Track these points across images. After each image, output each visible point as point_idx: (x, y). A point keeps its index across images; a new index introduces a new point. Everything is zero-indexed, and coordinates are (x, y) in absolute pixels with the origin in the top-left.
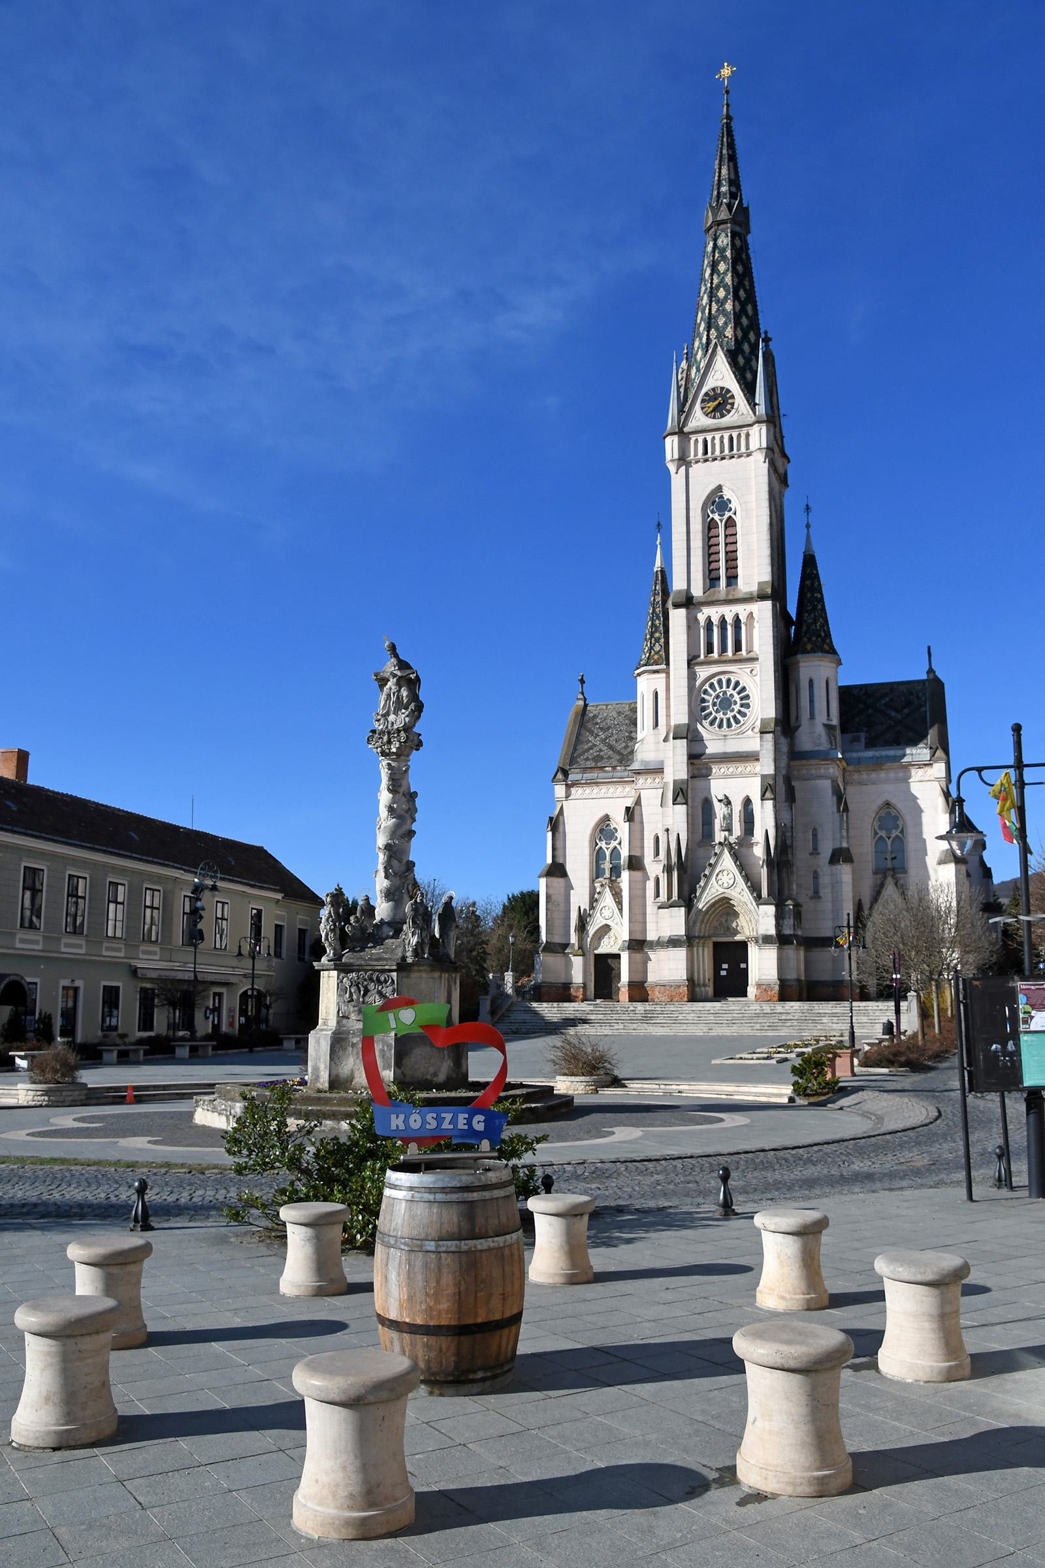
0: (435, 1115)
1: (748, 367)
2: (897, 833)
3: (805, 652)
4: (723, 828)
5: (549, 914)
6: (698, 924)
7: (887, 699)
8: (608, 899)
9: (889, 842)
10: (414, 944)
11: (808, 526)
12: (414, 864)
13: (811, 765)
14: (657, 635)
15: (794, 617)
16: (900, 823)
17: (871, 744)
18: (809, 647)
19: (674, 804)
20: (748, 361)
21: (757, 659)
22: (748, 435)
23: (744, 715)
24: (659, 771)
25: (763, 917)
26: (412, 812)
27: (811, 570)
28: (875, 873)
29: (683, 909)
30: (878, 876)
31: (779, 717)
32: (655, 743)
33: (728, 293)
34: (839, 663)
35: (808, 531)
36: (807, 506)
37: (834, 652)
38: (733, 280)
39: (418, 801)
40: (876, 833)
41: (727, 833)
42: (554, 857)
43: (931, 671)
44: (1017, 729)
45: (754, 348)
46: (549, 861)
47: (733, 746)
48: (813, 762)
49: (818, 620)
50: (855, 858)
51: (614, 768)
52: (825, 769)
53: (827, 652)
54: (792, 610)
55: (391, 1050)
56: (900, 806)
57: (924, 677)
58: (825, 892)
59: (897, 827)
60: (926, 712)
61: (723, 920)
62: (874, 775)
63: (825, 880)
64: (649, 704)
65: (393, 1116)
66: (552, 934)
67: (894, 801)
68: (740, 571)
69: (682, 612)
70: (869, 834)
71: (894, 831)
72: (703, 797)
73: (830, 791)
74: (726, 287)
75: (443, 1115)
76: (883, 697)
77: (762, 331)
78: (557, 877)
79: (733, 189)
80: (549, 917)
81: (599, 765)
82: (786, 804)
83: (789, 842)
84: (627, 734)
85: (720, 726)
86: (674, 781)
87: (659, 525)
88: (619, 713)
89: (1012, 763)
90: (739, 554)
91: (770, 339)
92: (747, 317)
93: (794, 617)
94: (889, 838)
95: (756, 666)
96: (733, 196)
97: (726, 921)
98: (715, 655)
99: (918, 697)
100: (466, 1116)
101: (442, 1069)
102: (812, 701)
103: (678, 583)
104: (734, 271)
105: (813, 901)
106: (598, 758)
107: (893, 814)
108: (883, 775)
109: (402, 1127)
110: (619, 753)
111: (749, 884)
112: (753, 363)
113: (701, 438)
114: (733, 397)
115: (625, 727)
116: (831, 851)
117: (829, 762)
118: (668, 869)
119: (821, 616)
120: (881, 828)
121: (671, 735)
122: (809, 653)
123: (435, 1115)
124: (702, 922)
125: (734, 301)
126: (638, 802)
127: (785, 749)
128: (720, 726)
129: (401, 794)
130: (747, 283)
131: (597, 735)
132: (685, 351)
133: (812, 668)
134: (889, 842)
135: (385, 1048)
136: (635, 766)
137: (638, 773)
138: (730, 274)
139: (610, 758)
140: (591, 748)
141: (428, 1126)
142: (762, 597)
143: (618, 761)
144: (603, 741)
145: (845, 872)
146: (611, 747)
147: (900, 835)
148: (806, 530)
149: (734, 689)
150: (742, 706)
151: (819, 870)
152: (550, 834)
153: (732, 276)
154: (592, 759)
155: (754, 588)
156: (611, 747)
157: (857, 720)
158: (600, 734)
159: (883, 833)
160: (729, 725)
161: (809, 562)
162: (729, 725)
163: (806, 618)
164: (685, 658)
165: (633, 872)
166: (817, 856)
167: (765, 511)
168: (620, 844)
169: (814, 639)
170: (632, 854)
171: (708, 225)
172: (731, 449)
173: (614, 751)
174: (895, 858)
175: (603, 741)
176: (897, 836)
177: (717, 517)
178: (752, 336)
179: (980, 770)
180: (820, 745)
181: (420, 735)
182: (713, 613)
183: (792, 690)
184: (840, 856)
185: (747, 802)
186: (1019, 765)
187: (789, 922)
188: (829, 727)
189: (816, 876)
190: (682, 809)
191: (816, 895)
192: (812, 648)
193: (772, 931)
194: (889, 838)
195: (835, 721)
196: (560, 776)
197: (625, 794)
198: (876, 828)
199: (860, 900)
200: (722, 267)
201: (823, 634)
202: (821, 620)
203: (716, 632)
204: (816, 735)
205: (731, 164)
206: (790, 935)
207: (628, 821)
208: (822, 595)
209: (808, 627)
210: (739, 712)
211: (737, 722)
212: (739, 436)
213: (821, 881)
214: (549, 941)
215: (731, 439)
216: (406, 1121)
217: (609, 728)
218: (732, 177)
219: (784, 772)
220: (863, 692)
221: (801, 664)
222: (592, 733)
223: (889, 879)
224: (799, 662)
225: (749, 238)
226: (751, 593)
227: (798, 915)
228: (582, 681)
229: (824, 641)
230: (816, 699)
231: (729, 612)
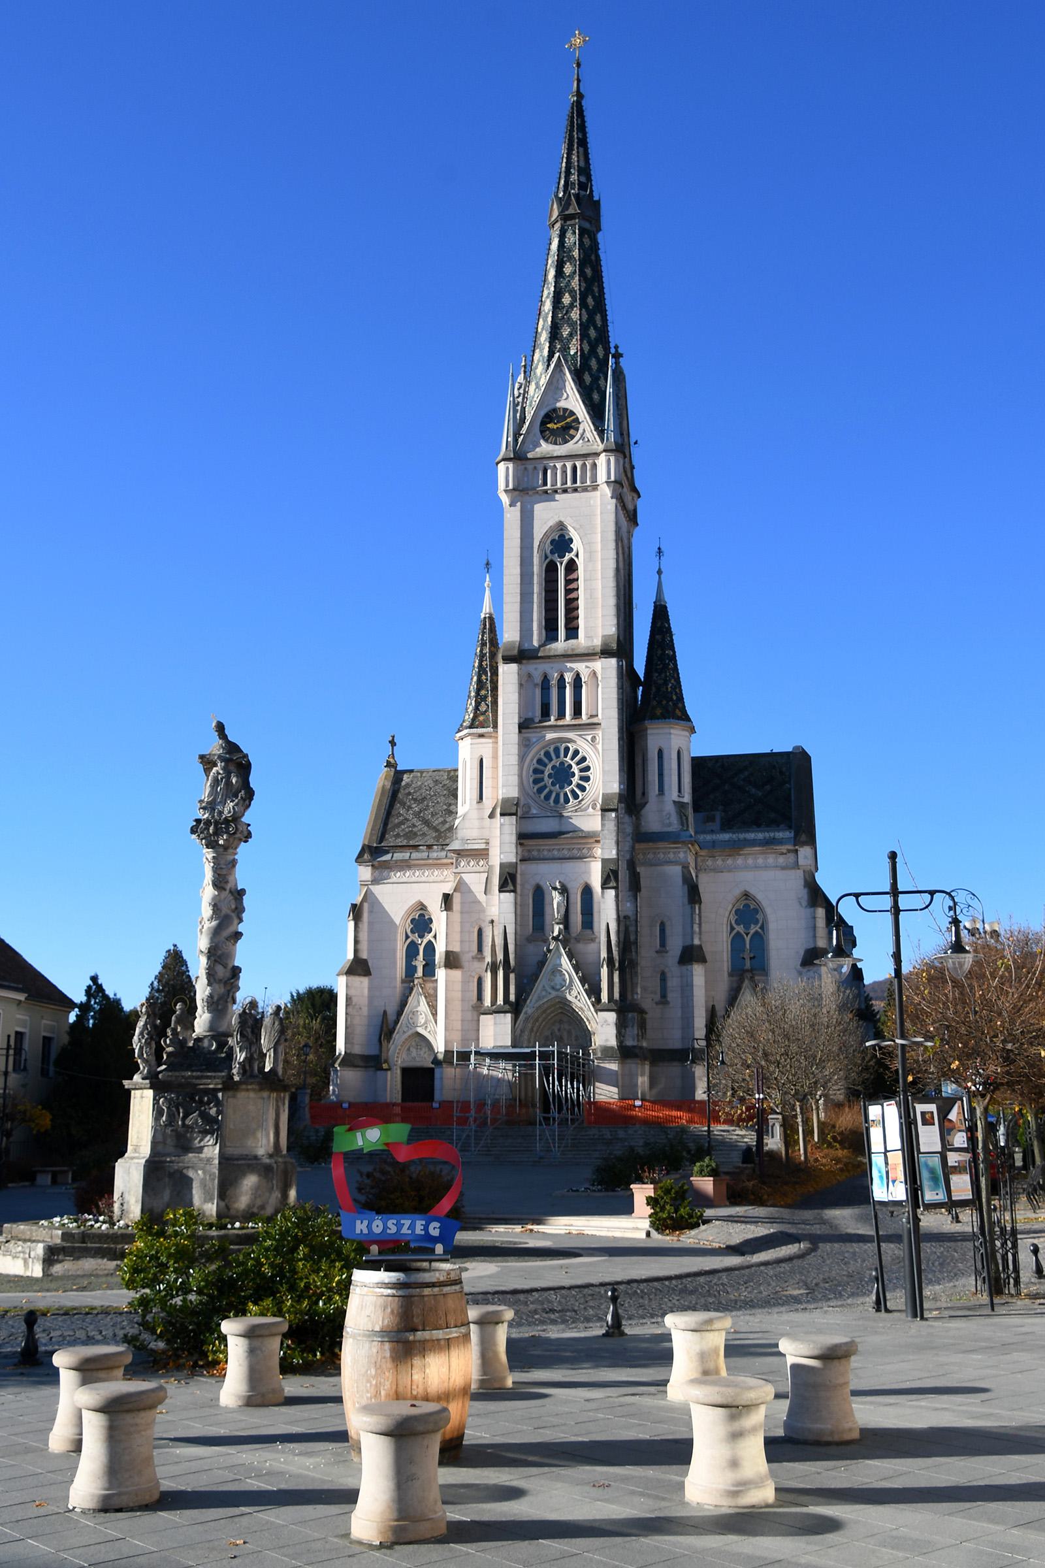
0: (395, 1222)
1: (595, 386)
2: (757, 928)
3: (654, 717)
4: (557, 921)
5: (349, 1019)
6: (526, 1033)
7: (746, 773)
9: (748, 939)
10: (241, 1060)
11: (659, 572)
12: (241, 969)
13: (658, 848)
14: (483, 692)
15: (642, 676)
16: (760, 917)
17: (727, 826)
19: (500, 891)
20: (595, 379)
22: (594, 465)
23: (583, 789)
24: (481, 854)
25: (602, 1026)
26: (239, 910)
27: (662, 623)
28: (731, 975)
29: (509, 1016)
30: (735, 978)
31: (623, 792)
32: (478, 819)
33: (574, 298)
34: (693, 730)
35: (660, 578)
36: (659, 549)
37: (688, 719)
38: (580, 285)
39: (246, 900)
40: (732, 929)
41: (561, 926)
42: (356, 951)
44: (893, 856)
45: (603, 364)
46: (350, 956)
48: (661, 845)
49: (670, 680)
50: (708, 957)
51: (430, 847)
52: (674, 853)
53: (679, 718)
54: (640, 666)
55: (214, 1179)
58: (673, 996)
59: (756, 922)
60: (790, 789)
61: (556, 1029)
62: (730, 861)
63: (673, 983)
65: (358, 1222)
66: (353, 1044)
68: (581, 622)
69: (514, 667)
70: (725, 929)
71: (752, 926)
72: (533, 883)
73: (679, 880)
74: (572, 292)
75: (402, 1222)
77: (612, 345)
78: (359, 975)
79: (583, 179)
80: (349, 1023)
81: (411, 843)
82: (631, 893)
83: (632, 938)
84: (445, 807)
86: (502, 865)
87: (488, 564)
88: (436, 782)
89: (888, 889)
90: (581, 602)
91: (621, 355)
92: (596, 328)
93: (642, 676)
94: (747, 934)
95: (599, 733)
96: (582, 186)
97: (559, 1030)
98: (552, 721)
99: (781, 773)
100: (424, 1223)
101: (270, 1201)
102: (661, 775)
103: (509, 634)
104: (582, 274)
105: (660, 1006)
106: (411, 835)
107: (752, 907)
108: (740, 861)
109: (365, 1231)
110: (436, 830)
111: (586, 986)
112: (602, 382)
114: (577, 420)
115: (443, 798)
116: (681, 948)
117: (680, 845)
119: (673, 677)
120: (737, 922)
121: (498, 811)
122: (658, 719)
123: (395, 1222)
124: (532, 1030)
125: (580, 310)
127: (629, 829)
129: (228, 891)
130: (596, 289)
132: (523, 364)
134: (748, 939)
135: (208, 1178)
137: (460, 853)
138: (577, 278)
139: (424, 834)
140: (402, 823)
141: (388, 1231)
142: (606, 652)
143: (434, 838)
144: (417, 814)
145: (698, 973)
146: (426, 823)
147: (760, 930)
148: (657, 576)
149: (572, 759)
150: (582, 778)
151: (666, 970)
152: (352, 924)
153: (580, 280)
154: (404, 835)
155: (597, 642)
156: (426, 823)
157: (712, 796)
158: (414, 806)
161: (660, 614)
163: (655, 678)
164: (516, 720)
165: (450, 971)
166: (664, 954)
167: (611, 554)
168: (435, 937)
169: (664, 702)
170: (450, 949)
171: (553, 219)
172: (574, 481)
173: (428, 826)
174: (754, 957)
175: (417, 814)
176: (757, 932)
178: (600, 351)
179: (857, 896)
180: (670, 825)
181: (249, 825)
183: (638, 761)
186: (895, 892)
187: (632, 1031)
188: (680, 806)
189: (663, 978)
190: (508, 897)
191: (663, 1000)
192: (661, 714)
193: (613, 1042)
194: (747, 934)
195: (687, 798)
196: (367, 856)
197: (442, 878)
198: (733, 922)
199: (713, 1006)
200: (568, 269)
201: (674, 698)
202: (673, 681)
204: (665, 813)
205: (581, 149)
206: (634, 1047)
207: (446, 910)
208: (674, 652)
210: (579, 786)
211: (576, 796)
212: (584, 465)
214: (348, 1051)
215: (574, 468)
216: (369, 1226)
217: (424, 799)
218: (582, 164)
219: (628, 857)
220: (719, 764)
221: (649, 732)
223: (746, 982)
224: (646, 729)
225: (600, 236)
227: (642, 1025)
228: (393, 743)
229: (675, 705)
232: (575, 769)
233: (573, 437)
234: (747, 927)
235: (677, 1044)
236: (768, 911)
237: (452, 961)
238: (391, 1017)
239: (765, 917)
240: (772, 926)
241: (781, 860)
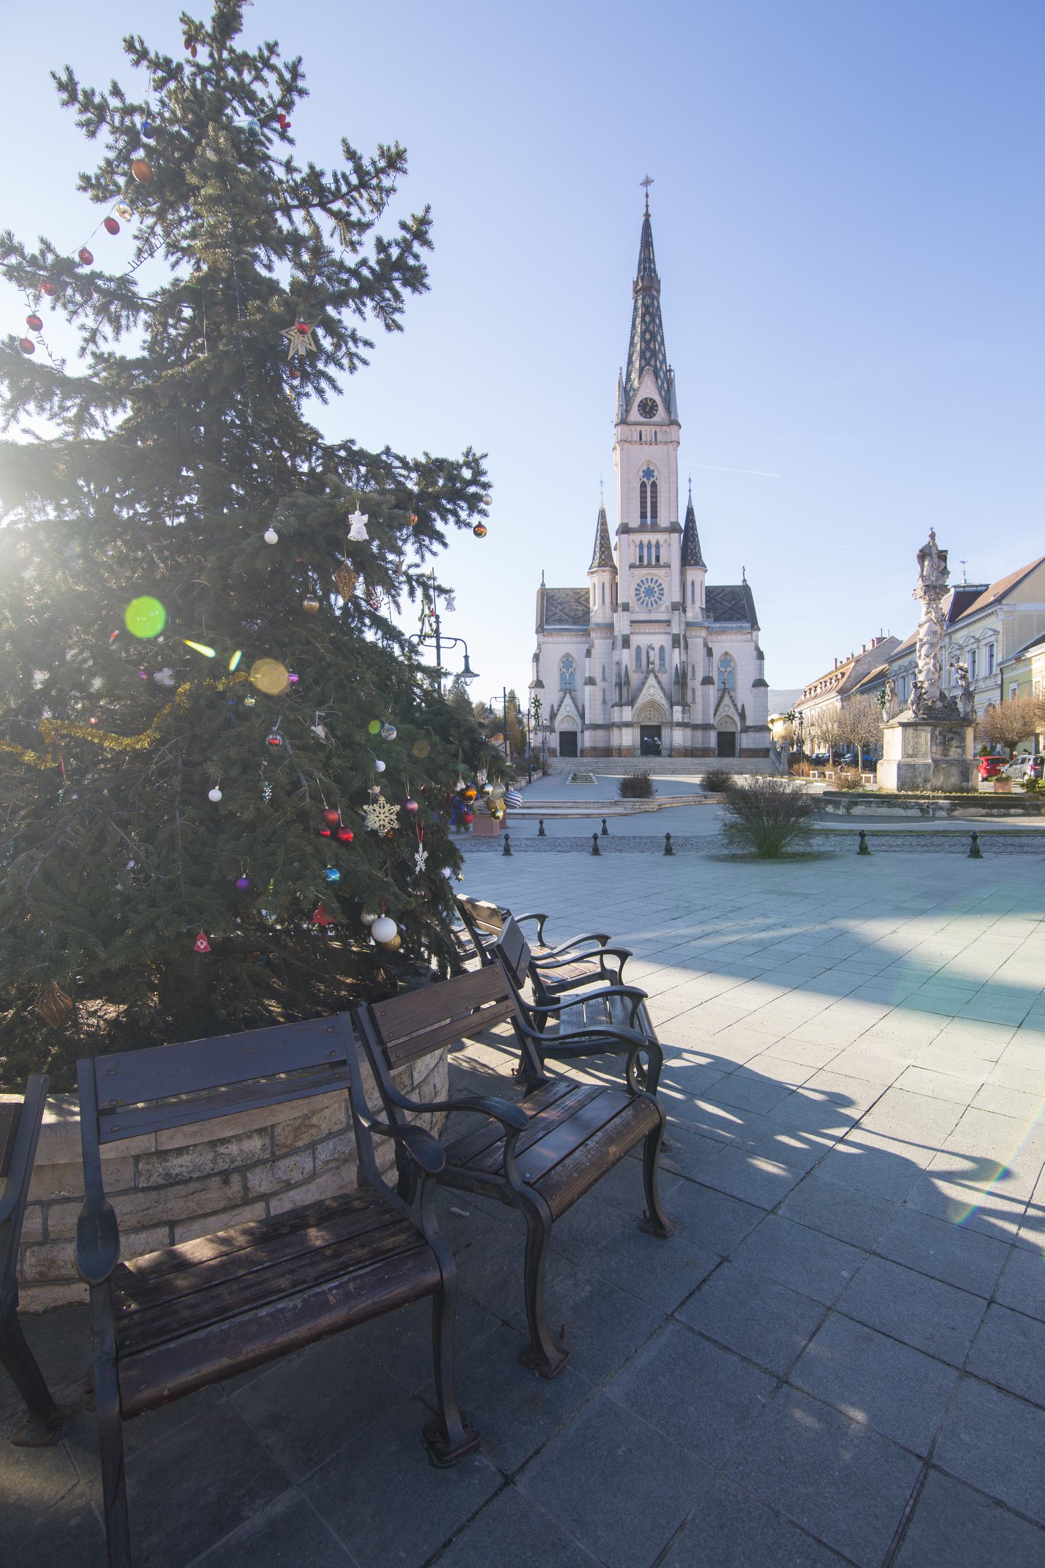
3: (690, 565)
8: (568, 700)
11: (690, 491)
17: (717, 619)
18: (692, 562)
20: (663, 383)
21: (669, 566)
43: (744, 581)
47: (654, 617)
48: (693, 628)
56: (733, 654)
57: (741, 584)
62: (719, 637)
64: (599, 591)
67: (730, 652)
70: (716, 669)
76: (721, 593)
85: (647, 605)
88: (567, 595)
102: (693, 594)
108: (724, 637)
113: (638, 428)
114: (657, 406)
118: (619, 685)
126: (593, 647)
128: (647, 605)
131: (556, 607)
133: (692, 574)
136: (591, 626)
144: (561, 610)
146: (566, 614)
156: (566, 614)
159: (722, 669)
160: (652, 605)
161: (690, 512)
162: (652, 605)
170: (592, 675)
175: (561, 610)
177: (645, 480)
178: (664, 366)
182: (646, 538)
184: (707, 681)
185: (662, 649)
188: (701, 608)
189: (694, 690)
195: (704, 607)
203: (645, 550)
209: (691, 550)
211: (657, 603)
213: (696, 694)
222: (553, 606)
223: (727, 694)
226: (666, 528)
230: (696, 592)
231: (653, 538)
232: (656, 589)
233: (654, 415)
234: (726, 668)
235: (700, 722)
236: (737, 661)
237: (591, 681)
238: (556, 708)
239: (735, 664)
240: (739, 668)
241: (744, 637)
